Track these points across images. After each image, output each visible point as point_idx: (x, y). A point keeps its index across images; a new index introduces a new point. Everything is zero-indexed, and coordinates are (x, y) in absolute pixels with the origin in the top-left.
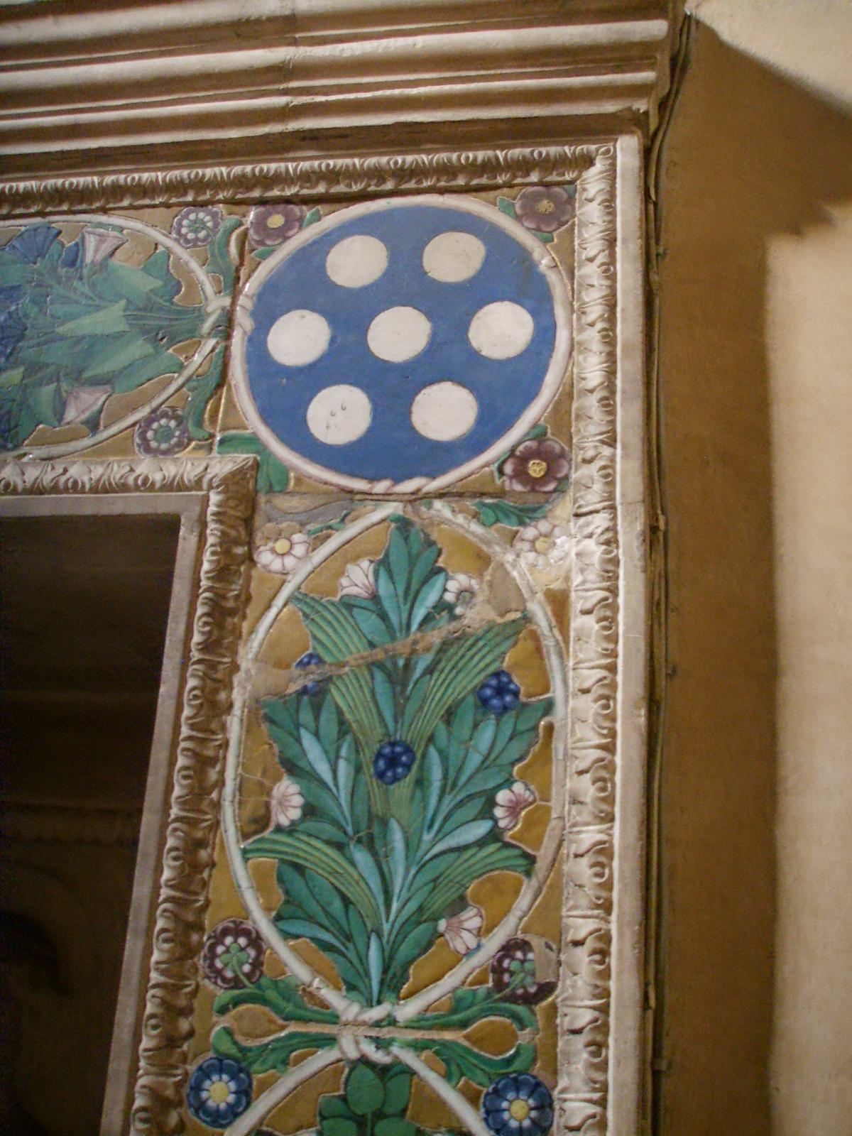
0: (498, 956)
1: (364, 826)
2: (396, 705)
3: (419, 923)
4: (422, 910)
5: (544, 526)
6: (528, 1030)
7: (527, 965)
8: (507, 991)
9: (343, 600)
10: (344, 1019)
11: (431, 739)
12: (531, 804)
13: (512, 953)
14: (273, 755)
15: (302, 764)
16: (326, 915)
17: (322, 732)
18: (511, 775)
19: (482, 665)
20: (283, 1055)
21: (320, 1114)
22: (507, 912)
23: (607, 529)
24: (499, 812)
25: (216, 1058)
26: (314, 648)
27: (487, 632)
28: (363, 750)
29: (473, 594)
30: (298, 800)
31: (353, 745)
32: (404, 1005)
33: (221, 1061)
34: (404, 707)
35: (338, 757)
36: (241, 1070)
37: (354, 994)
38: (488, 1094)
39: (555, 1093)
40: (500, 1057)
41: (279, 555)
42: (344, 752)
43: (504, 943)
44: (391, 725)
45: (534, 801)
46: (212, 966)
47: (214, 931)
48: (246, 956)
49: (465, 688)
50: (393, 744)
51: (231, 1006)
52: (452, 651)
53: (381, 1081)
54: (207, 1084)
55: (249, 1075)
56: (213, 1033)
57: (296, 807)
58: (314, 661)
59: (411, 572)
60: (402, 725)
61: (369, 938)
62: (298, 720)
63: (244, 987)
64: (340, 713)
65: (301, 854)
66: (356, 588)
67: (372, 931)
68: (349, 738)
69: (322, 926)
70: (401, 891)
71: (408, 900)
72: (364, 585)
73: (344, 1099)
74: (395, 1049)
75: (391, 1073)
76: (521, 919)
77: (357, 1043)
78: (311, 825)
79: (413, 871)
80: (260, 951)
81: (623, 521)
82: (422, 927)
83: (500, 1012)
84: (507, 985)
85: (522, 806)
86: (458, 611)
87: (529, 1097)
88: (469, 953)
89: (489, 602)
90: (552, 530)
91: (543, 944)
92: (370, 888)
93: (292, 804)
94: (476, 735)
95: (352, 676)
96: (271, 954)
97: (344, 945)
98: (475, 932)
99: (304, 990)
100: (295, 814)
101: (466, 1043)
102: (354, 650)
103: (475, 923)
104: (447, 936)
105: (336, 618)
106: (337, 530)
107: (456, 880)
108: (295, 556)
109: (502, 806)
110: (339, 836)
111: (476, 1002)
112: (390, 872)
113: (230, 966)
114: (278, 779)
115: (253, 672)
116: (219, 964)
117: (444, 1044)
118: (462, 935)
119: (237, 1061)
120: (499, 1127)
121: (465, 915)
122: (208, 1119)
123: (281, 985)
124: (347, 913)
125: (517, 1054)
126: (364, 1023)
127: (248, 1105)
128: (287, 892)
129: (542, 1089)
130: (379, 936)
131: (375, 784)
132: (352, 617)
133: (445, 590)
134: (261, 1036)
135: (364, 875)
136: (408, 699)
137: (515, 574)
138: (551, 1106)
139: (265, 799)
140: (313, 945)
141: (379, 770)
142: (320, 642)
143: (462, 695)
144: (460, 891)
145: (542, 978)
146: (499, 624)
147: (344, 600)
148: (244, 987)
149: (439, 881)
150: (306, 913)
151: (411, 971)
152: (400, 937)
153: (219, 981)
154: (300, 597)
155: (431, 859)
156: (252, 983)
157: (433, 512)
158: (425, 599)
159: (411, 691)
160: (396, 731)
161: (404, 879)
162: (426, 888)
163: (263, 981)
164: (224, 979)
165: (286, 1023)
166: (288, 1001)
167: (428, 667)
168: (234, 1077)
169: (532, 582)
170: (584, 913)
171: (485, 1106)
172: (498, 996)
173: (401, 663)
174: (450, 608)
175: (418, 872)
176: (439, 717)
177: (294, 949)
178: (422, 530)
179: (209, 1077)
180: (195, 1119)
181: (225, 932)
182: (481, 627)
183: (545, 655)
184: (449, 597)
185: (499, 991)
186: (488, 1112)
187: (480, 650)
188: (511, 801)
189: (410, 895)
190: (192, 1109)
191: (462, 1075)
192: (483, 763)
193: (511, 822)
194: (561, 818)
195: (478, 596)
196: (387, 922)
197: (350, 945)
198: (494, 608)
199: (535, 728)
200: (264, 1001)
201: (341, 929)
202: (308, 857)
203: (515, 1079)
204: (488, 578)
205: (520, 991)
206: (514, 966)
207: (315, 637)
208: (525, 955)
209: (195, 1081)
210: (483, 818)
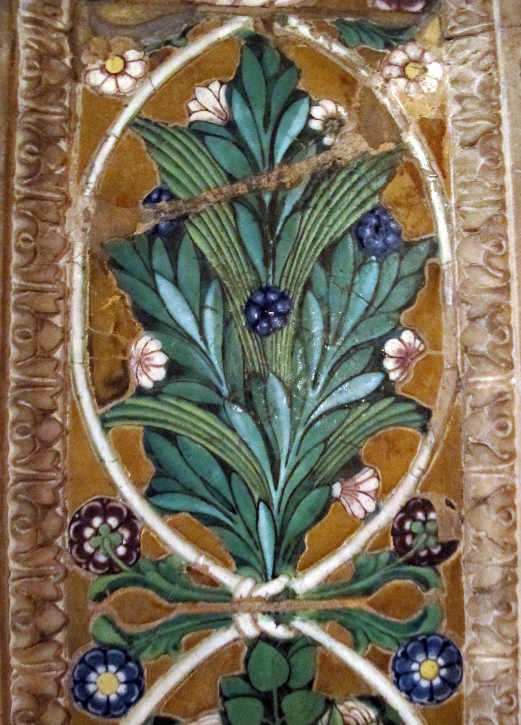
0: (398, 518)
1: (240, 385)
2: (265, 245)
3: (311, 489)
4: (314, 473)
5: (413, 51)
6: (432, 592)
7: (429, 526)
8: (411, 553)
9: (193, 127)
10: (237, 596)
11: (308, 285)
12: (421, 353)
13: (412, 514)
14: (126, 307)
15: (162, 316)
16: (205, 485)
17: (182, 279)
18: (398, 324)
19: (358, 201)
20: (174, 640)
21: (221, 694)
22: (405, 471)
23: (487, 53)
24: (389, 364)
25: (99, 649)
26: (163, 182)
27: (360, 165)
28: (232, 299)
29: (342, 123)
30: (161, 359)
31: (220, 293)
32: (303, 577)
33: (105, 652)
34: (274, 248)
35: (202, 307)
36: (128, 659)
37: (247, 571)
38: (396, 658)
39: (463, 650)
40: (407, 620)
41: (110, 74)
42: (209, 301)
43: (403, 504)
44: (261, 269)
45: (424, 351)
46: (81, 551)
47: (79, 512)
48: (119, 537)
49: (342, 227)
50: (266, 290)
51: (108, 592)
52: (324, 185)
53: (285, 657)
54: (93, 676)
55: (138, 663)
56: (91, 624)
57: (158, 366)
58: (164, 198)
59: (268, 97)
60: (274, 271)
61: (257, 509)
62: (151, 266)
63: (121, 571)
64: (201, 257)
65: (171, 420)
66: (207, 113)
67: (260, 500)
68: (214, 286)
69: (203, 499)
70: (288, 455)
71: (298, 464)
72: (216, 109)
73: (246, 678)
74: (298, 624)
75: (294, 648)
76: (419, 478)
77: (255, 621)
78: (177, 386)
79: (300, 433)
80: (134, 531)
81: (503, 46)
82: (315, 493)
83: (405, 575)
84: (409, 548)
85: (414, 355)
86: (327, 140)
87: (439, 656)
88: (368, 517)
89: (358, 130)
90: (422, 54)
91: (444, 501)
92: (253, 455)
93: (153, 363)
94: (357, 279)
95: (210, 214)
96: (147, 533)
97: (230, 518)
98: (373, 495)
99: (189, 569)
100: (159, 374)
101: (371, 610)
102: (211, 184)
103: (372, 485)
104: (343, 501)
105: (188, 149)
106: (178, 47)
107: (348, 441)
108: (130, 76)
109: (392, 357)
110: (215, 399)
111: (378, 567)
112: (274, 435)
113: (101, 550)
114: (133, 335)
115: (92, 211)
116: (88, 548)
117: (348, 613)
118: (359, 498)
119: (125, 652)
120: (410, 688)
121: (360, 477)
122: (100, 712)
123: (163, 566)
124: (229, 482)
125: (424, 616)
126: (259, 599)
127: (141, 694)
128: (158, 464)
129: (451, 648)
130: (269, 506)
131: (249, 337)
132: (205, 145)
133: (310, 117)
134: (144, 622)
135: (245, 439)
136: (279, 239)
137: (385, 101)
138: (460, 662)
139: (121, 357)
140: (194, 520)
141: (251, 321)
142: (170, 175)
143: (339, 235)
144: (353, 453)
145: (444, 537)
146: (373, 157)
147: (193, 127)
148: (121, 571)
149: (329, 442)
150: (183, 486)
151: (306, 540)
152: (291, 506)
153: (91, 567)
154: (141, 123)
155: (320, 417)
156: (130, 566)
157: (287, 29)
158: (289, 126)
159: (282, 230)
160: (268, 276)
161: (292, 441)
162: (317, 449)
163: (142, 563)
164: (97, 565)
165: (173, 605)
166: (173, 583)
167: (298, 203)
168: (121, 667)
169: (405, 112)
170: (487, 468)
171: (394, 669)
172: (401, 560)
173: (267, 198)
174: (317, 136)
175: (305, 434)
176: (315, 259)
177: (174, 526)
178: (278, 49)
179: (94, 669)
180: (84, 712)
181: (92, 512)
182: (354, 159)
183: (425, 190)
184: (316, 125)
185: (401, 555)
186: (398, 675)
187: (354, 184)
188: (400, 351)
189: (297, 459)
190: (80, 703)
191: (369, 641)
192: (367, 309)
193: (402, 374)
194: (455, 367)
195: (348, 125)
196: (276, 488)
197: (237, 517)
198: (366, 139)
199: (421, 270)
200: (146, 585)
201: (225, 501)
202: (179, 422)
203: (424, 641)
204: (356, 104)
205: (424, 553)
206: (417, 527)
207: (162, 170)
208: (426, 515)
209: (79, 675)
210: (372, 371)
